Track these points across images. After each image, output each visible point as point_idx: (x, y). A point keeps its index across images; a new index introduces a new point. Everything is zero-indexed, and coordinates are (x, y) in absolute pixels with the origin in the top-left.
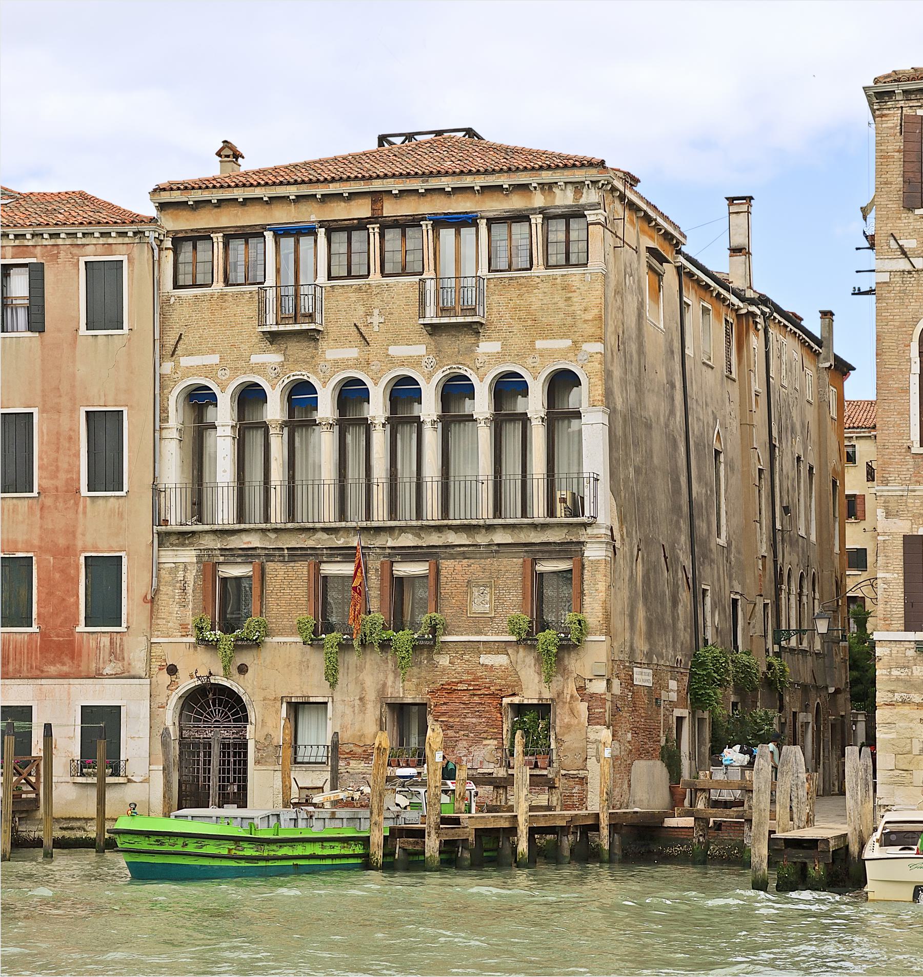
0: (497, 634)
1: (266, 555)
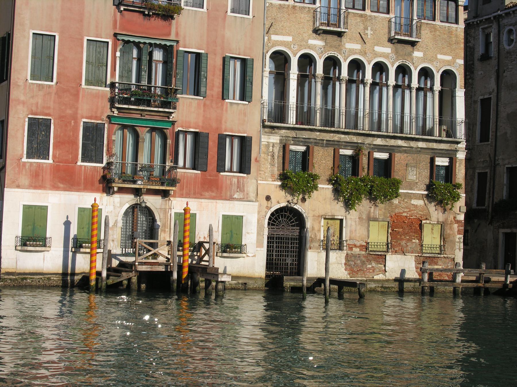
0: (419, 190)
1: (315, 143)
